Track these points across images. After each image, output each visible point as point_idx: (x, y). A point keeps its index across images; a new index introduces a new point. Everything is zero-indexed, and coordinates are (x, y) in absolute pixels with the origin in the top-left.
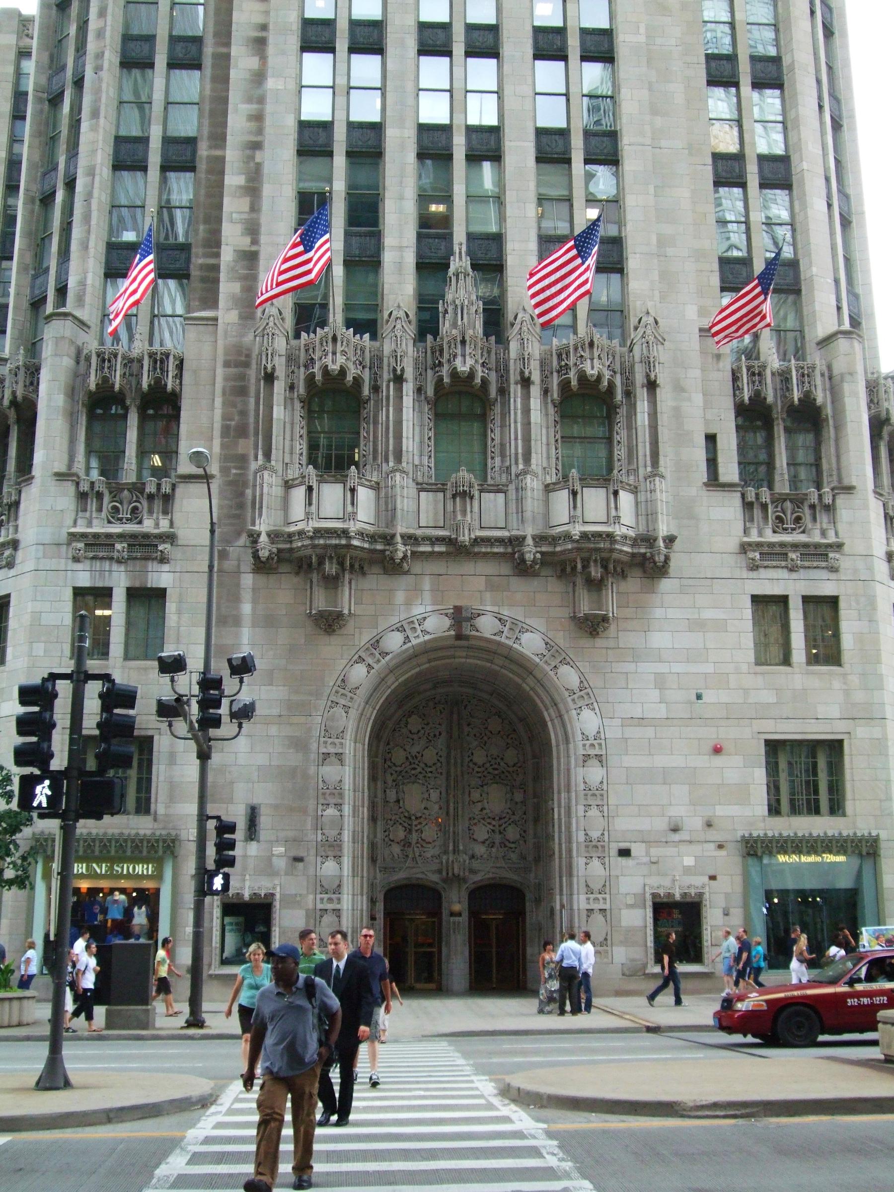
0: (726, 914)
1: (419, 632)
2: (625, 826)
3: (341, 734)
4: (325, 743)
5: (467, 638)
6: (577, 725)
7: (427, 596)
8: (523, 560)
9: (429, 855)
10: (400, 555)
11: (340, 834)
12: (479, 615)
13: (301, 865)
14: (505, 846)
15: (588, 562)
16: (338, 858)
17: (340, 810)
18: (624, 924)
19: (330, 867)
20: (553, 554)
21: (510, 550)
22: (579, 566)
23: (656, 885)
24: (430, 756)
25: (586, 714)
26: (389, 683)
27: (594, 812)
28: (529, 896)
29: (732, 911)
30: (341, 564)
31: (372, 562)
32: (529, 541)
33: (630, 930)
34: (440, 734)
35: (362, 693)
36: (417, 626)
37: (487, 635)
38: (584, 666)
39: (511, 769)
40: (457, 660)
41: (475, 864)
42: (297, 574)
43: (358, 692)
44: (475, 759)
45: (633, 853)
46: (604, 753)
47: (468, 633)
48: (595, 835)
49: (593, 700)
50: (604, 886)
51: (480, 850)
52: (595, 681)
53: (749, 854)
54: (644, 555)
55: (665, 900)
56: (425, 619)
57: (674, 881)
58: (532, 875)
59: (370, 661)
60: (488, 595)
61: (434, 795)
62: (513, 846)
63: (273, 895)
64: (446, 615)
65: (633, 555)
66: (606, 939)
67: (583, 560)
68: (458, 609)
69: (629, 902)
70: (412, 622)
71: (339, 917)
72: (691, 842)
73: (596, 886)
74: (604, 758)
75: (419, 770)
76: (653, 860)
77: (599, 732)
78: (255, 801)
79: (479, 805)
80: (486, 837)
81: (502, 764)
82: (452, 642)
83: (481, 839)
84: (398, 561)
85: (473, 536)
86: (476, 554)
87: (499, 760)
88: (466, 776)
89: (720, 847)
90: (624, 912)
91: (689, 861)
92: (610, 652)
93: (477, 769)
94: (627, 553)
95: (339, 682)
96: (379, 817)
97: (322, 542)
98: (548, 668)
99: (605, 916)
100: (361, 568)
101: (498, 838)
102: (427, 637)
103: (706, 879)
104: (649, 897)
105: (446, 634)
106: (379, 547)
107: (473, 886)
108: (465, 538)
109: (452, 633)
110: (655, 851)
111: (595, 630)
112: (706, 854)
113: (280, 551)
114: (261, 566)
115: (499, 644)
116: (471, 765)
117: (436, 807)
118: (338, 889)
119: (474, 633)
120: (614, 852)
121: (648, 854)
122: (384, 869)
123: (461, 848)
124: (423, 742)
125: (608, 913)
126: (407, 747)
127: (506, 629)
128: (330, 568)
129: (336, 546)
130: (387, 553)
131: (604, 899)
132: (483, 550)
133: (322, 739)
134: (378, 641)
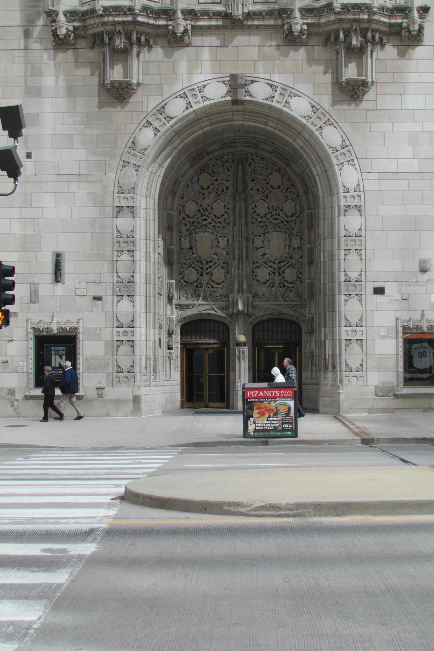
1: (199, 98)
3: (133, 190)
4: (119, 197)
5: (242, 103)
6: (340, 179)
7: (207, 65)
8: (290, 31)
9: (218, 294)
10: (181, 29)
11: (132, 276)
12: (253, 82)
13: (100, 302)
14: (284, 286)
15: (349, 32)
16: (131, 297)
17: (133, 256)
18: (377, 352)
19: (125, 305)
20: (318, 25)
21: (280, 22)
22: (342, 35)
23: (407, 318)
24: (218, 208)
25: (347, 168)
26: (175, 144)
27: (353, 256)
28: (304, 329)
30: (129, 37)
31: (157, 36)
32: (297, 14)
34: (227, 189)
35: (151, 153)
36: (197, 92)
37: (260, 99)
38: (347, 127)
39: (289, 219)
40: (235, 123)
41: (258, 302)
42: (92, 48)
43: (146, 153)
44: (258, 210)
45: (386, 291)
46: (362, 203)
47: (243, 98)
48: (353, 275)
49: (354, 157)
51: (262, 290)
52: (355, 139)
54: (400, 25)
56: (204, 86)
57: (423, 315)
58: (307, 311)
59: (156, 124)
60: (260, 64)
61: (223, 243)
62: (291, 285)
63: (76, 328)
64: (224, 82)
65: (391, 25)
66: (362, 365)
67: (344, 31)
68: (234, 77)
69: (383, 333)
70: (193, 89)
71: (133, 346)
73: (354, 320)
74: (363, 208)
75: (209, 220)
76: (404, 297)
77: (358, 185)
78: (60, 250)
79: (262, 251)
80: (268, 277)
81: (281, 214)
82: (230, 107)
83: (263, 280)
84: (179, 35)
85: (246, 11)
86: (251, 27)
87: (279, 211)
88: (250, 226)
92: (369, 113)
93: (259, 219)
94: (385, 23)
95: (130, 144)
96: (175, 262)
97: (111, 19)
98: (313, 129)
99: (361, 346)
100: (147, 41)
101: (277, 279)
102: (207, 103)
105: (224, 99)
106: (162, 22)
107: (256, 321)
108: (239, 12)
109: (229, 98)
111: (356, 94)
113: (75, 28)
114: (60, 43)
115: (271, 107)
116: (254, 215)
117: (224, 253)
118: (131, 324)
119: (248, 98)
120: (370, 290)
122: (180, 307)
123: (245, 287)
124: (212, 196)
125: (364, 342)
126: (199, 201)
127: (277, 95)
128: (120, 43)
129: (124, 22)
130: (171, 27)
132: (256, 23)
133: (116, 195)
134: (163, 107)
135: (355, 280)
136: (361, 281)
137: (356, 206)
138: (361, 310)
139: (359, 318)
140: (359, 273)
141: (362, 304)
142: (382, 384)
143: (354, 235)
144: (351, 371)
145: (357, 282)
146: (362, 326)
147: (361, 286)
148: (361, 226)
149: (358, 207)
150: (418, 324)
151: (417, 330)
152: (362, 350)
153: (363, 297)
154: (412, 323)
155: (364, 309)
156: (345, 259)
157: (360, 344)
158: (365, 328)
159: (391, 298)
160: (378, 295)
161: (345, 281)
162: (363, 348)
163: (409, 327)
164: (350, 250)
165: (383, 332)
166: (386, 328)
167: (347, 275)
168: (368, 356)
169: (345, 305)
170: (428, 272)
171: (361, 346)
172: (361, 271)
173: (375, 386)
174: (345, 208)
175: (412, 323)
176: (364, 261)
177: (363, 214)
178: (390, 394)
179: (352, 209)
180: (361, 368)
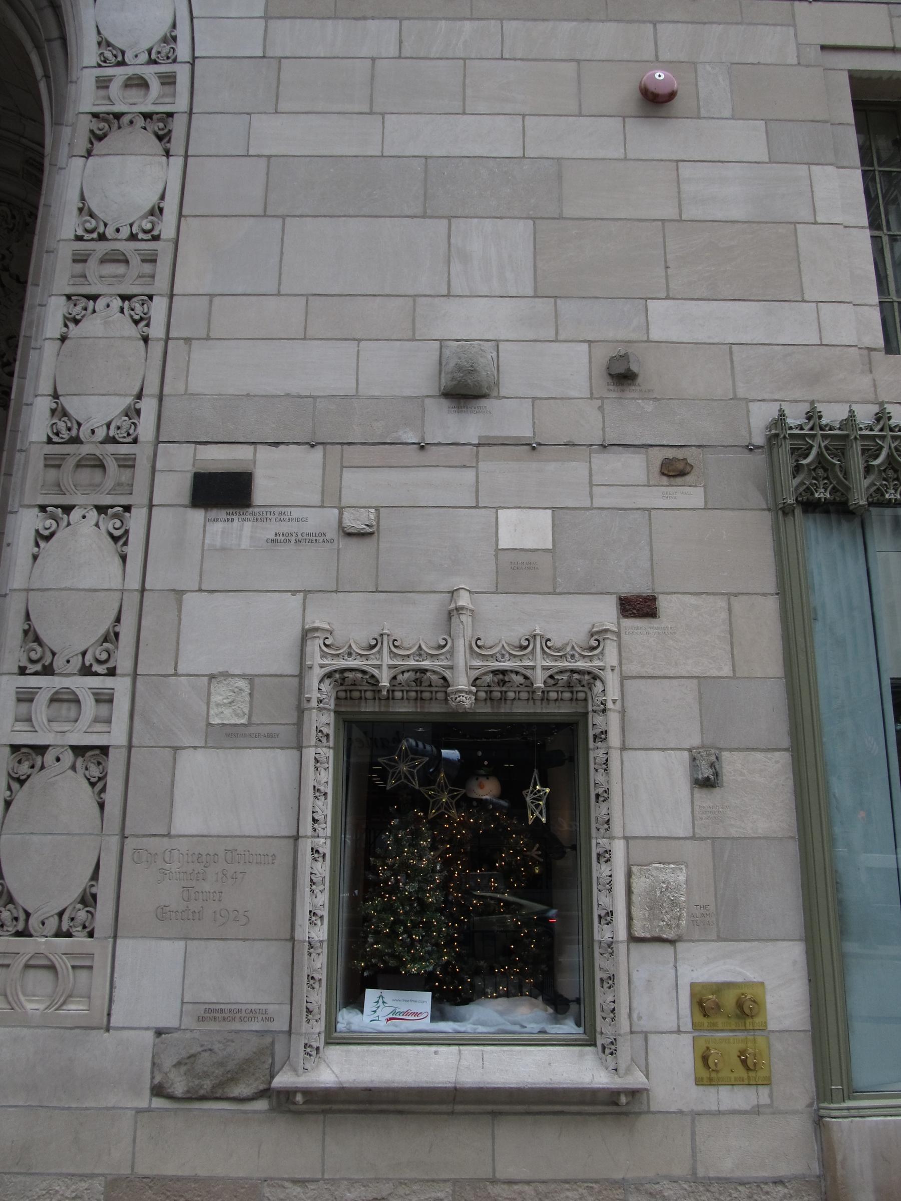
0: (707, 783)
2: (240, 366)
18: (188, 820)
27: (107, 324)
29: (733, 765)
33: (220, 858)
48: (96, 411)
50: (112, 637)
53: (810, 506)
55: (403, 708)
57: (452, 614)
66: (88, 900)
72: (533, 447)
73: (70, 637)
74: (178, 126)
76: (355, 521)
77: (171, 39)
89: (674, 471)
90: (198, 768)
91: (524, 529)
99: (98, 784)
103: (606, 613)
104: (319, 690)
110: (367, 488)
112: (605, 498)
120: (174, 485)
121: (331, 496)
125: (115, 764)
131: (105, 699)
135: (101, 434)
136: (135, 441)
137: (147, 116)
138: (116, 583)
139: (101, 631)
140: (129, 400)
141: (124, 558)
142: (201, 1019)
143: (125, 232)
144: (24, 933)
145: (111, 448)
146: (112, 672)
147: (127, 463)
148: (162, 197)
149: (160, 127)
150: (426, 663)
151: (419, 699)
152: (102, 806)
153: (136, 522)
154: (387, 660)
155: (134, 583)
156: (63, 339)
157: (95, 772)
158: (128, 681)
159: (285, 527)
160: (214, 513)
161: (50, 441)
162: (107, 797)
163: (374, 681)
164: (94, 298)
165: (228, 705)
166: (243, 684)
167: (65, 414)
168: (130, 844)
169: (35, 557)
170: (483, 402)
171: (98, 784)
172: (139, 396)
173: (159, 1033)
174: (95, 125)
175: (387, 660)
176: (156, 349)
177: (177, 145)
178: (242, 1089)
179: (127, 130)
180: (82, 915)
